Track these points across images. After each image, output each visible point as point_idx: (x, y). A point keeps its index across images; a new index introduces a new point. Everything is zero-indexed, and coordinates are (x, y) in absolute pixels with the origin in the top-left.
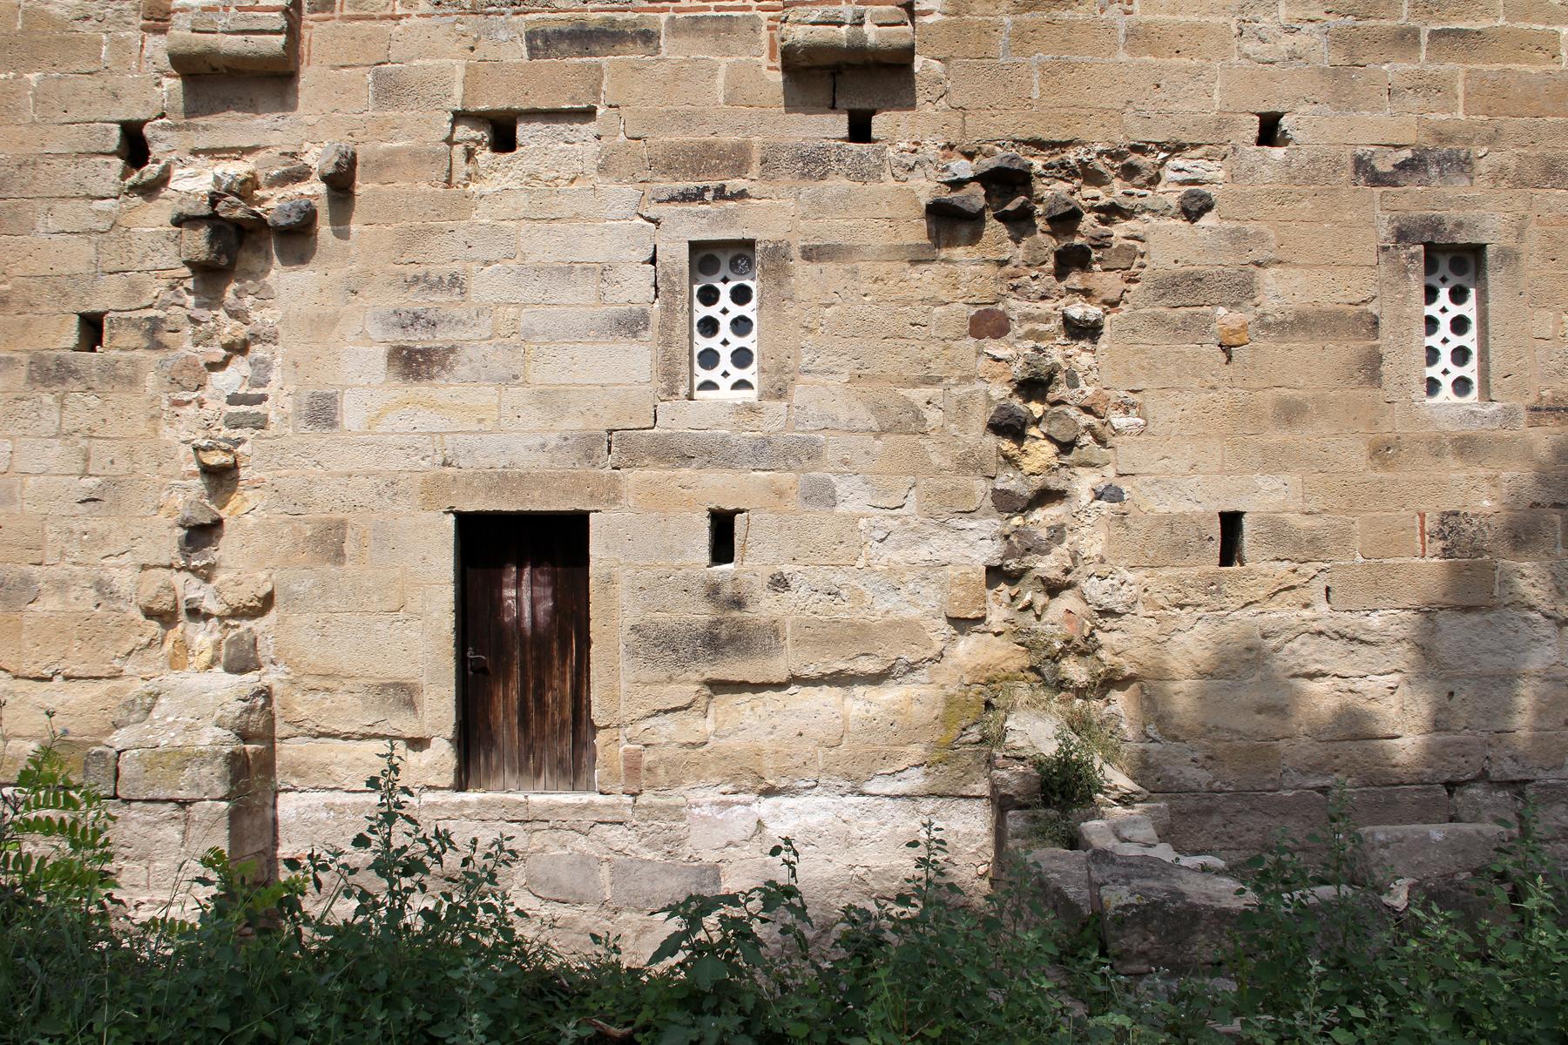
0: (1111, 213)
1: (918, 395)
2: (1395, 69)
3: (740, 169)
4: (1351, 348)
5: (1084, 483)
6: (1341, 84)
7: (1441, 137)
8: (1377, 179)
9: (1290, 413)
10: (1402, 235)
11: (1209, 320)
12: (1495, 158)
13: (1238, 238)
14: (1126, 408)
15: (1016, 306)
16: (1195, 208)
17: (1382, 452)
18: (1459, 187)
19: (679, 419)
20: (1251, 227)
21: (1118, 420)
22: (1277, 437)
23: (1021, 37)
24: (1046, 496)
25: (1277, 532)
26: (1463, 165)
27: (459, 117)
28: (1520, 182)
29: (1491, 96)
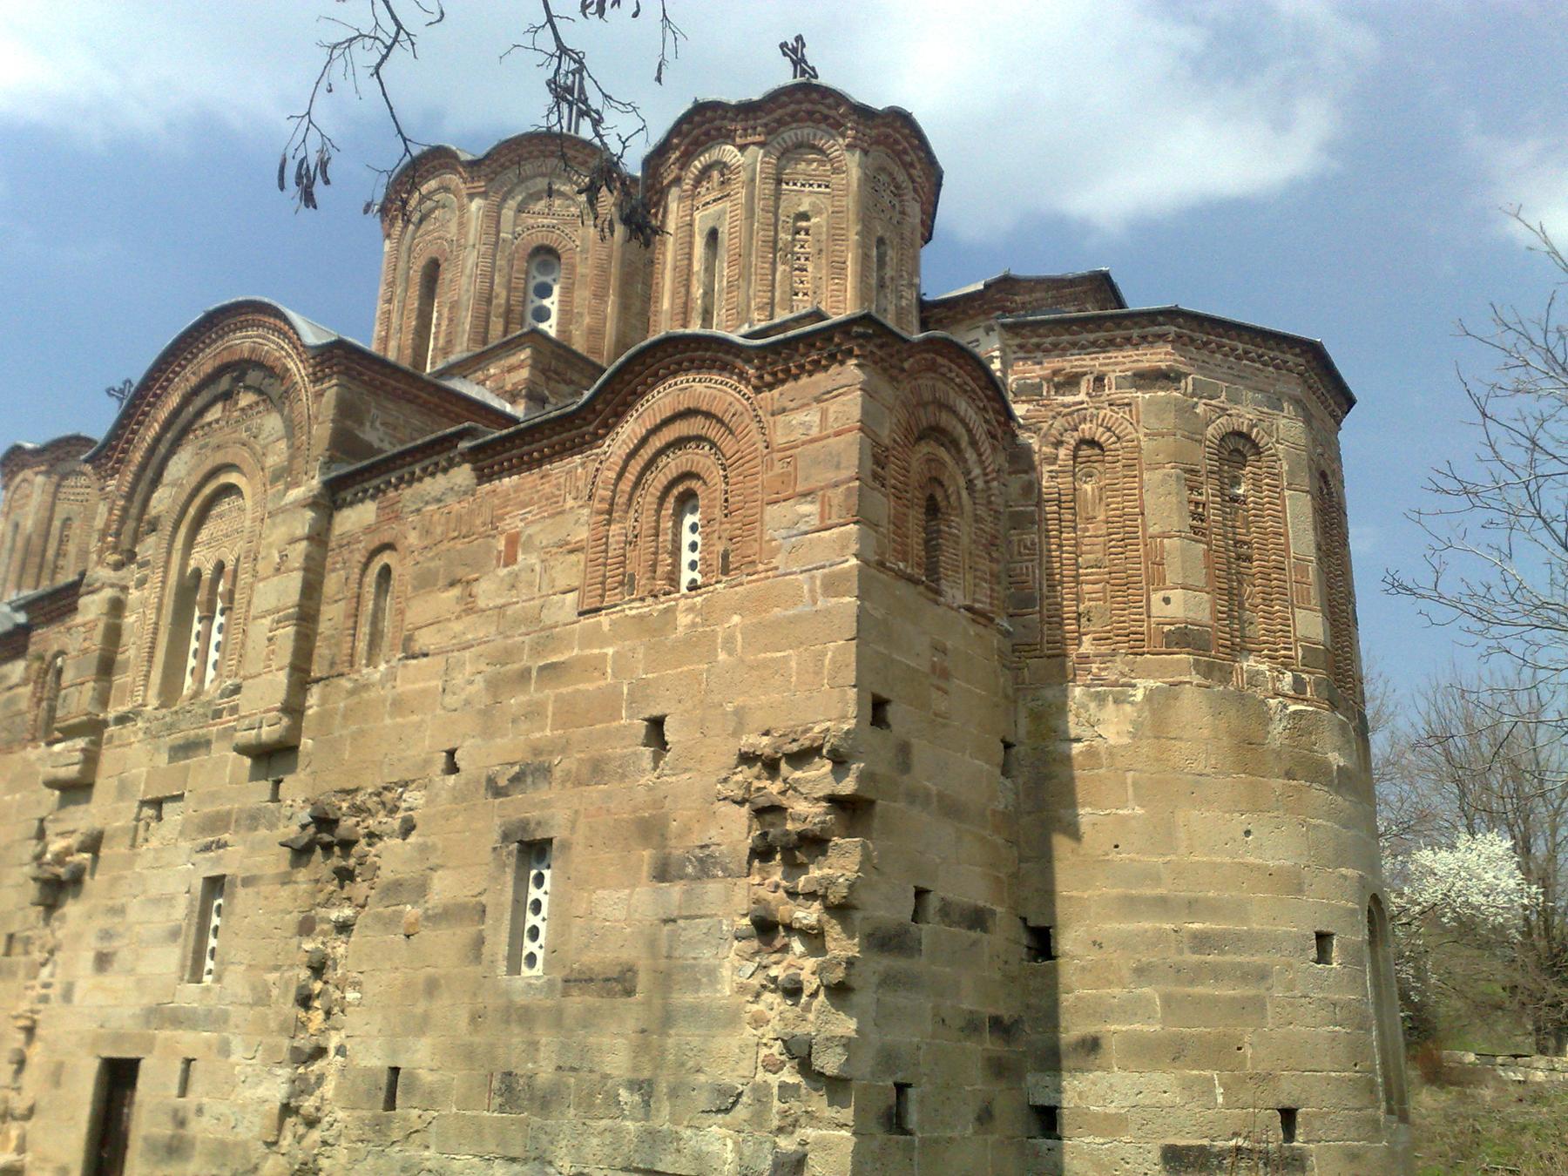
0: (372, 836)
1: (272, 977)
2: (515, 702)
3: (226, 829)
6: (488, 719)
7: (537, 751)
8: (498, 792)
10: (506, 837)
11: (400, 914)
12: (566, 764)
13: (424, 849)
14: (356, 985)
16: (408, 828)
18: (544, 793)
19: (189, 996)
20: (430, 841)
21: (351, 995)
26: (545, 772)
27: (144, 803)
28: (579, 783)
29: (569, 713)
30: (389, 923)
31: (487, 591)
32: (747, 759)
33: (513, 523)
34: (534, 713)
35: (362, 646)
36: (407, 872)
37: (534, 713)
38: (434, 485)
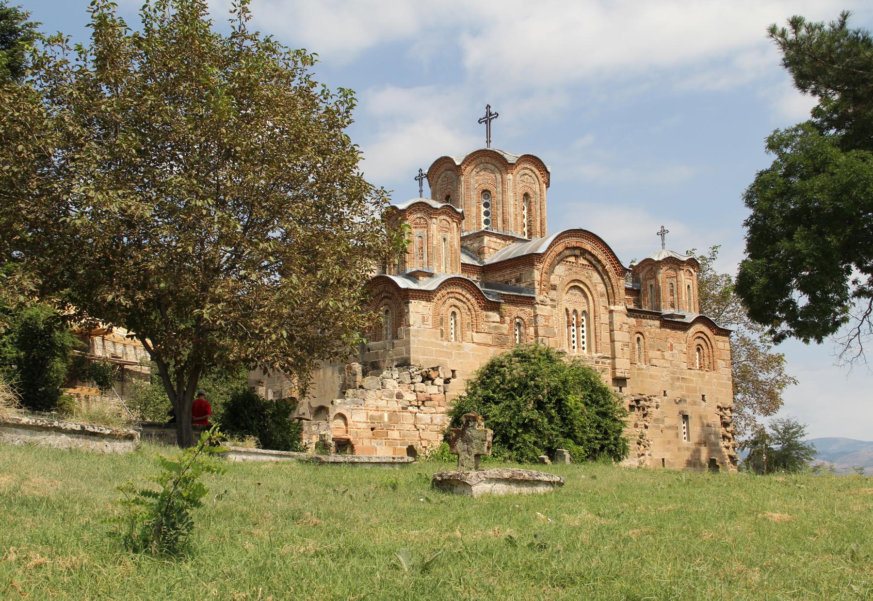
0: (649, 407)
2: (677, 384)
4: (675, 432)
5: (647, 453)
9: (669, 442)
15: (639, 423)
17: (679, 449)
18: (685, 405)
22: (668, 446)
23: (638, 375)
24: (643, 455)
25: (669, 462)
30: (658, 427)
31: (667, 354)
32: (718, 407)
33: (670, 340)
35: (637, 357)
37: (681, 387)
38: (651, 322)
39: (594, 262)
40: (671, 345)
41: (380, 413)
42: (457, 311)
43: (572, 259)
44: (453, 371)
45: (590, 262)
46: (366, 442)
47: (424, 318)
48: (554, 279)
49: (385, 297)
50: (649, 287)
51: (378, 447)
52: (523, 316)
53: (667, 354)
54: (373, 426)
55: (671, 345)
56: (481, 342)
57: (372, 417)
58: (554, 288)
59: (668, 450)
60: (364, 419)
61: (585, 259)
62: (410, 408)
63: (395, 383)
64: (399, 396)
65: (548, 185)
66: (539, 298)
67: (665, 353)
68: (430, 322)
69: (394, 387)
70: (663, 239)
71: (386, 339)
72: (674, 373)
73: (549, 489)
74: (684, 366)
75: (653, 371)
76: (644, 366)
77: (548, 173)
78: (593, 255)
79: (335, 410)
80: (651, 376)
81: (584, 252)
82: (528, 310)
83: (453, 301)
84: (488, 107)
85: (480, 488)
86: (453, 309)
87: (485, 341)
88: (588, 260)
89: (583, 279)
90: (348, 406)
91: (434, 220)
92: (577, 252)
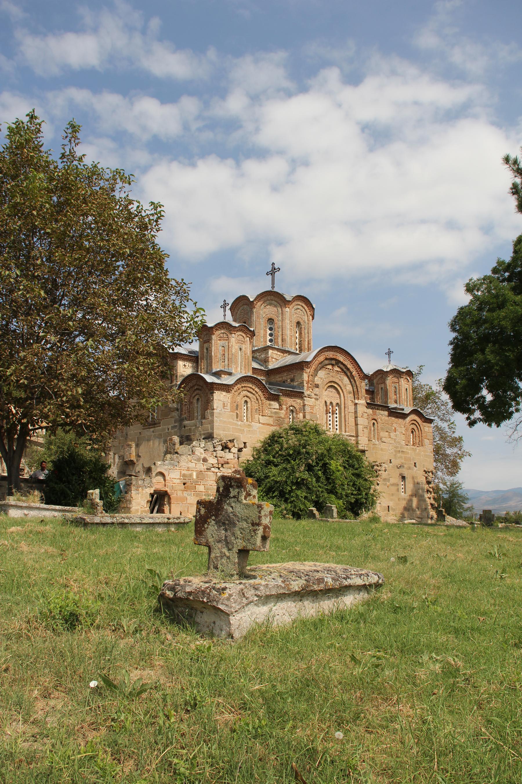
4: (396, 488)
9: (393, 495)
17: (399, 499)
18: (404, 470)
25: (392, 508)
30: (385, 484)
31: (392, 434)
32: (424, 471)
33: (395, 425)
34: (401, 457)
35: (372, 436)
36: (387, 477)
37: (401, 457)
38: (382, 412)
39: (345, 370)
40: (395, 428)
41: (190, 472)
42: (248, 400)
43: (330, 367)
44: (245, 443)
45: (342, 370)
46: (180, 493)
47: (224, 404)
48: (317, 380)
49: (197, 389)
50: (380, 389)
51: (188, 497)
52: (295, 405)
53: (392, 434)
54: (185, 481)
55: (395, 428)
56: (265, 422)
57: (184, 475)
58: (317, 386)
59: (391, 500)
60: (178, 477)
61: (339, 367)
62: (213, 469)
63: (202, 451)
64: (205, 460)
65: (313, 318)
66: (306, 393)
67: (391, 434)
68: (229, 407)
69: (201, 454)
70: (389, 357)
71: (197, 419)
72: (397, 447)
73: (363, 596)
74: (403, 443)
75: (383, 446)
76: (377, 443)
77: (313, 308)
78: (344, 365)
79: (156, 469)
80: (382, 449)
81: (338, 362)
82: (299, 401)
83: (245, 393)
84: (273, 264)
85: (245, 618)
86: (246, 398)
87: (268, 422)
88: (341, 368)
89: (337, 381)
90: (166, 467)
91: (233, 335)
92: (333, 362)
